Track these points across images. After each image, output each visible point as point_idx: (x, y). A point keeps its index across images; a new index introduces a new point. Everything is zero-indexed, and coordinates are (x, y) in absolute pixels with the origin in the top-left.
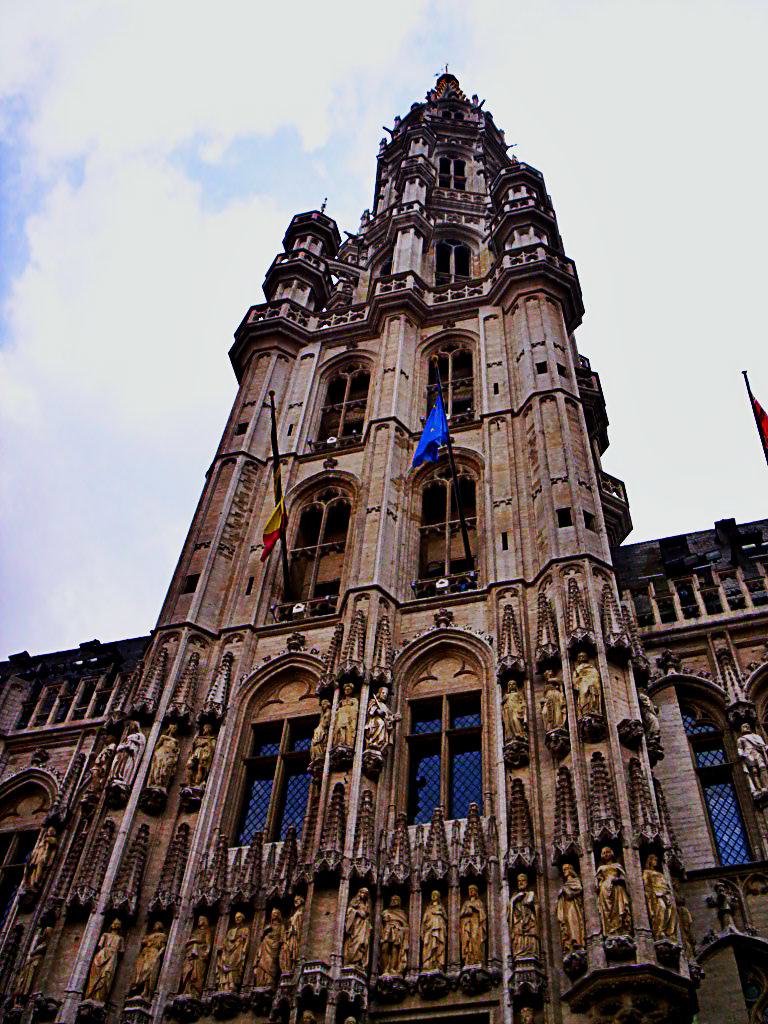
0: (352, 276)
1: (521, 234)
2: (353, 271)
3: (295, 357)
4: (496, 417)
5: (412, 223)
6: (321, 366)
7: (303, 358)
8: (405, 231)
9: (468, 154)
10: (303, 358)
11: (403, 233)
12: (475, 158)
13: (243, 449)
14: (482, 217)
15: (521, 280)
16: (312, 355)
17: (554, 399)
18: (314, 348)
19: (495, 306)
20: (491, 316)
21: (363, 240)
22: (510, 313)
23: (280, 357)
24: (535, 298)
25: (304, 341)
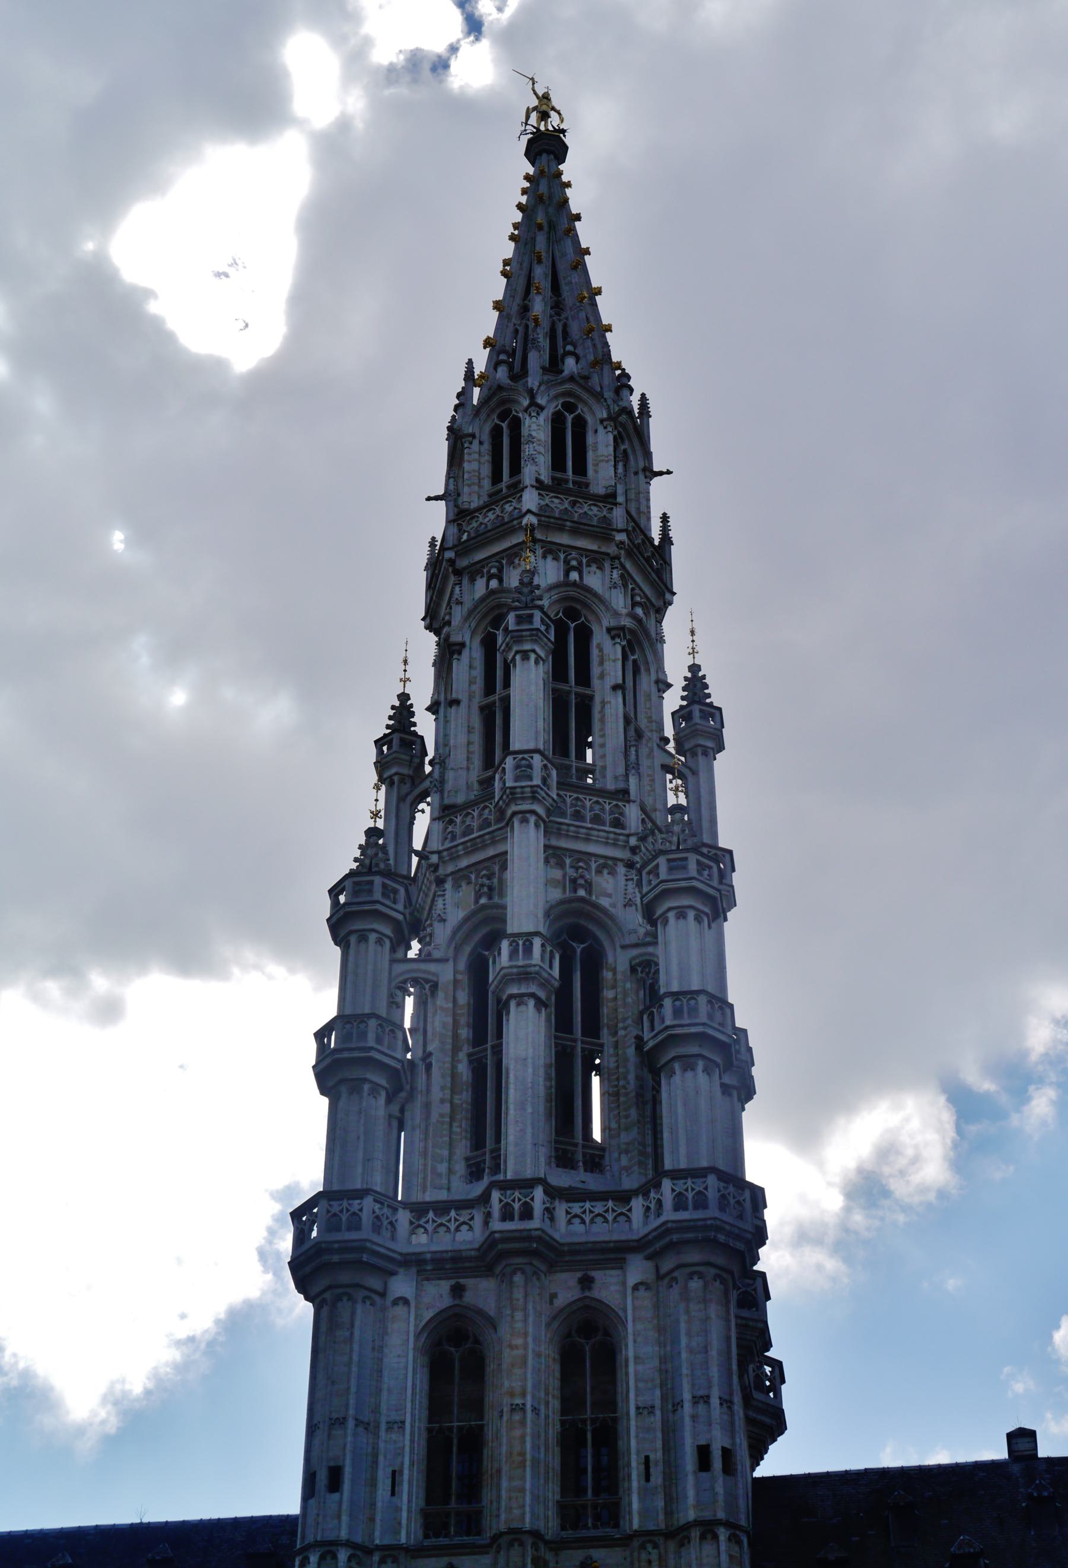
0: (427, 981)
1: (685, 1070)
2: (429, 972)
3: (383, 1295)
4: (647, 1536)
5: (533, 989)
6: (420, 1333)
7: (396, 1302)
8: (521, 999)
9: (600, 610)
10: (396, 1302)
11: (518, 1004)
12: (609, 630)
13: (344, 1535)
14: (621, 860)
15: (687, 1242)
16: (405, 1301)
17: (715, 1537)
18: (402, 1286)
19: (648, 1258)
20: (641, 1283)
21: (436, 867)
22: (666, 1280)
23: (365, 1299)
24: (701, 1276)
25: (391, 1266)
